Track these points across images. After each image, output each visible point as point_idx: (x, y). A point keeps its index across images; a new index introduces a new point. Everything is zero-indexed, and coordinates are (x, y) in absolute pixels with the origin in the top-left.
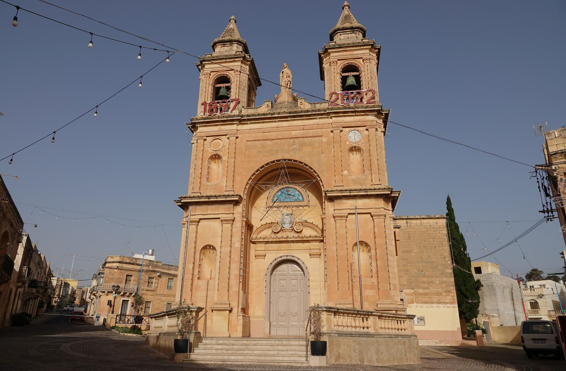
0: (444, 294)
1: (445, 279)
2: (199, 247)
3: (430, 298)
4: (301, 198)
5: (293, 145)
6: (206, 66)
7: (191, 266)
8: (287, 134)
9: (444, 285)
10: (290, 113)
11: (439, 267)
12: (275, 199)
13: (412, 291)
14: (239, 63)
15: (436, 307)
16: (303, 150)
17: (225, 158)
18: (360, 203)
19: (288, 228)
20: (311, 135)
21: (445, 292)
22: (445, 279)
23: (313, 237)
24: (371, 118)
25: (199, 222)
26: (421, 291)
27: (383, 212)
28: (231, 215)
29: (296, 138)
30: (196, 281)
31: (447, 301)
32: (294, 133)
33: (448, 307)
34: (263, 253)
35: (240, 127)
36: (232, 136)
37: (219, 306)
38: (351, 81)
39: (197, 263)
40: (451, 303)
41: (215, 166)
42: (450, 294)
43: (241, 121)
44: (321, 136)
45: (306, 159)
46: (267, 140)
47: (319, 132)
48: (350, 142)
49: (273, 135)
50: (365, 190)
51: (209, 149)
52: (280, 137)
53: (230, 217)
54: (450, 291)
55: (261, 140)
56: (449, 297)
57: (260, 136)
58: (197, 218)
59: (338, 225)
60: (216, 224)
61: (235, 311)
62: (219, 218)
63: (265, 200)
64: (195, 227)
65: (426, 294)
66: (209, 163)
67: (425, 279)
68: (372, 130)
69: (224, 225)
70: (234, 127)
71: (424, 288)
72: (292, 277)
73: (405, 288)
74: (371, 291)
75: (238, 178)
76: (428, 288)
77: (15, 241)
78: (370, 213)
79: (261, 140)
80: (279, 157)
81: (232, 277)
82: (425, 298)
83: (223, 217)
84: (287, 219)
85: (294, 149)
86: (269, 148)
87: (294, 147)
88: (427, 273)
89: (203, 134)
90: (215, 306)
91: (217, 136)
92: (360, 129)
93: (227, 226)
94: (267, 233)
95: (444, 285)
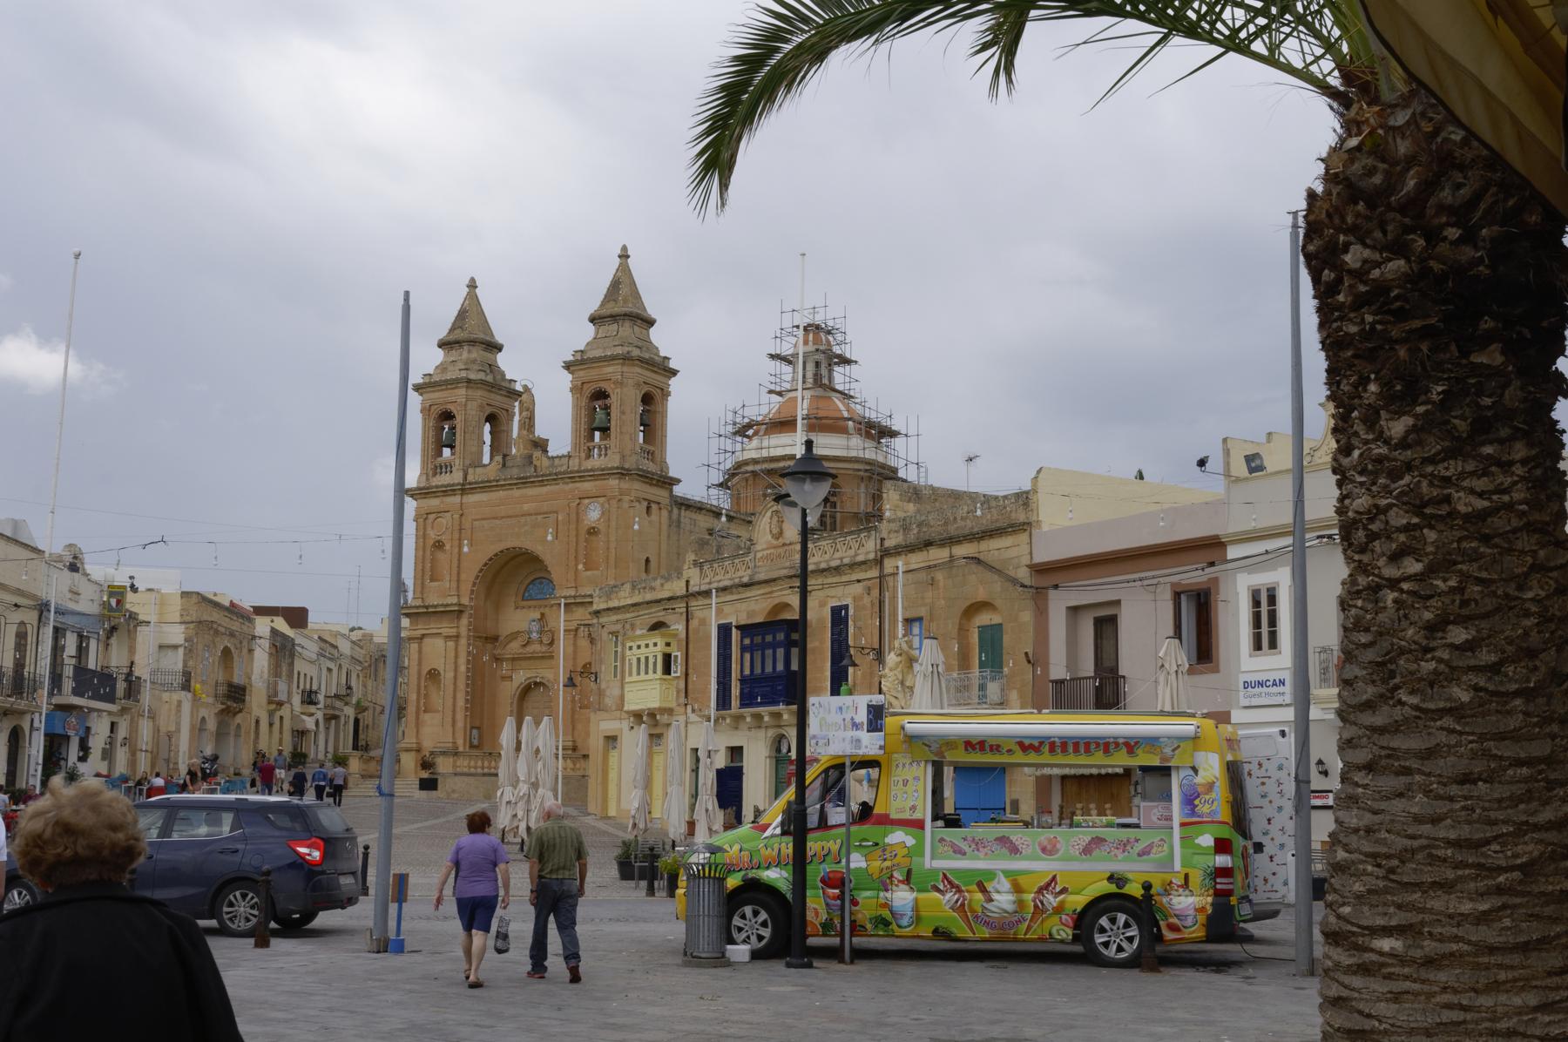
14: (463, 391)
17: (448, 547)
24: (613, 482)
32: (526, 507)
39: (423, 692)
41: (440, 556)
43: (465, 488)
53: (453, 632)
58: (418, 633)
60: (439, 642)
68: (614, 502)
70: (457, 499)
75: (463, 576)
80: (509, 544)
84: (535, 627)
92: (602, 500)
93: (451, 644)
94: (514, 647)
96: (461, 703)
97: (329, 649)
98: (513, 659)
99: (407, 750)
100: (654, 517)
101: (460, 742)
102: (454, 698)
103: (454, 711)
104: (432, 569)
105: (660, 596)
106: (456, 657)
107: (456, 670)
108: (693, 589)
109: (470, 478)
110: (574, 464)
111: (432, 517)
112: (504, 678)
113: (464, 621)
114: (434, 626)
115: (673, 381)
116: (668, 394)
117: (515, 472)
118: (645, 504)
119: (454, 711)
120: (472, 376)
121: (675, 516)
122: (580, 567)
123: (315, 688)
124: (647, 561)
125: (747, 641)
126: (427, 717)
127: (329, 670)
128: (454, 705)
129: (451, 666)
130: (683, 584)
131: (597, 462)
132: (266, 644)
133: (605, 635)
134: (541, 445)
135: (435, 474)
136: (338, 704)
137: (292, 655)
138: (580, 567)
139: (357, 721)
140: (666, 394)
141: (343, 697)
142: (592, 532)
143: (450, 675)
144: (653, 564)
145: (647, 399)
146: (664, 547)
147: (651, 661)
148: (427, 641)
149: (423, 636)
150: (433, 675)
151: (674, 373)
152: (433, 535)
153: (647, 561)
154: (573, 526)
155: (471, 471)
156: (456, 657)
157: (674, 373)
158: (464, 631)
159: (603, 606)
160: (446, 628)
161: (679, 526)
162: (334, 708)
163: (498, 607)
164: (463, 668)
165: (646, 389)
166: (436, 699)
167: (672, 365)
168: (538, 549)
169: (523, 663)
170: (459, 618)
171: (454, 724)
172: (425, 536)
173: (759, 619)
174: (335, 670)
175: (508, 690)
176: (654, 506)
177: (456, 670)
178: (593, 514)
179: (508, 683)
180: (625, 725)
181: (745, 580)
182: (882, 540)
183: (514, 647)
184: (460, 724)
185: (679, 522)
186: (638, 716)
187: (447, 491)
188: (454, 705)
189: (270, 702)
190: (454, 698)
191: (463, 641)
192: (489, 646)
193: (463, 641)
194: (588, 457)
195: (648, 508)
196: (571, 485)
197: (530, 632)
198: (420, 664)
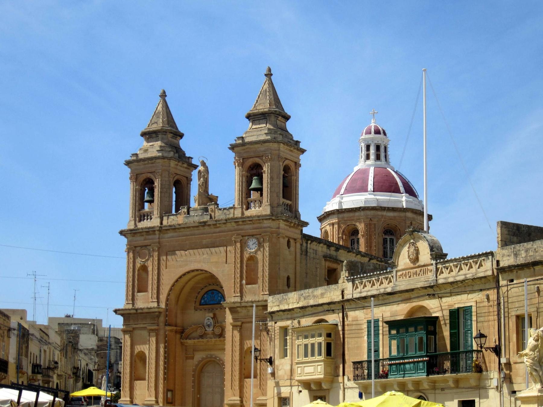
17: (150, 269)
25: (132, 331)
77: (6, 338)
92: (258, 236)
100: (292, 248)
105: (321, 301)
108: (346, 297)
109: (165, 222)
110: (238, 213)
111: (138, 249)
112: (187, 358)
113: (162, 319)
115: (302, 157)
116: (300, 166)
117: (196, 219)
118: (287, 239)
120: (166, 155)
121: (304, 248)
122: (244, 282)
123: (38, 362)
124: (288, 278)
125: (394, 332)
126: (138, 383)
127: (45, 351)
130: (340, 293)
131: (254, 211)
133: (277, 328)
134: (213, 200)
135: (140, 221)
138: (244, 282)
140: (297, 165)
142: (252, 258)
144: (292, 281)
145: (286, 169)
146: (298, 268)
147: (316, 346)
148: (137, 332)
151: (303, 151)
153: (288, 278)
155: (165, 218)
157: (303, 151)
158: (162, 324)
159: (275, 309)
161: (306, 255)
163: (184, 309)
165: (287, 162)
167: (302, 146)
168: (214, 270)
170: (158, 317)
173: (401, 317)
176: (291, 241)
179: (190, 361)
180: (295, 389)
181: (389, 290)
182: (498, 262)
184: (161, 389)
185: (307, 252)
186: (306, 385)
187: (150, 231)
191: (162, 333)
194: (248, 208)
195: (289, 242)
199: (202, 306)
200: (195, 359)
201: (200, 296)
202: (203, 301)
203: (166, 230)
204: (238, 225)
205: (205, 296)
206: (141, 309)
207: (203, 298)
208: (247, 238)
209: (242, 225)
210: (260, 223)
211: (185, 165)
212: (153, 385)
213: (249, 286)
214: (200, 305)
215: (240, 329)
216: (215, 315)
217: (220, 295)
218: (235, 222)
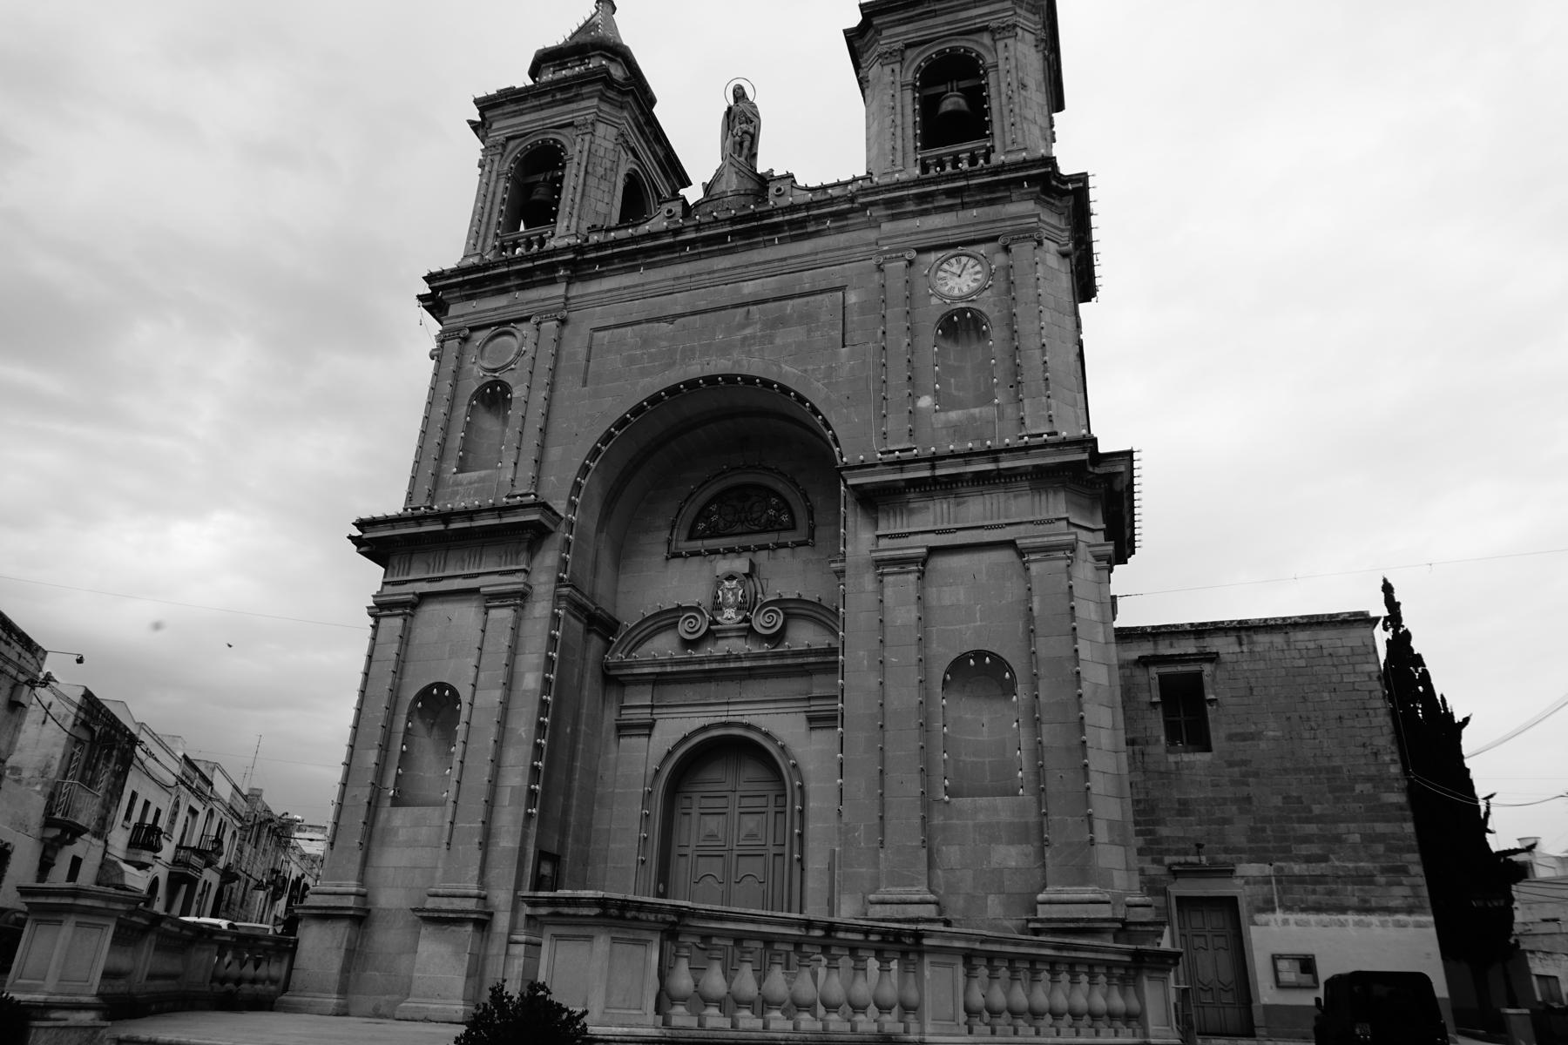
0: (1381, 879)
1: (1381, 827)
2: (410, 693)
3: (1330, 893)
4: (785, 518)
5: (743, 327)
6: (495, 126)
7: (372, 757)
8: (725, 294)
9: (1380, 848)
10: (733, 220)
11: (1359, 788)
12: (701, 526)
13: (1267, 870)
15: (1357, 924)
16: (778, 341)
17: (518, 392)
18: (977, 509)
19: (729, 624)
20: (807, 287)
21: (1384, 871)
22: (1381, 827)
23: (817, 652)
26: (1298, 869)
27: (1060, 534)
28: (520, 578)
29: (756, 303)
30: (385, 810)
31: (1392, 904)
32: (749, 288)
33: (1399, 925)
34: (643, 715)
35: (577, 289)
36: (548, 319)
37: (444, 904)
38: (953, 102)
39: (398, 746)
40: (1410, 911)
41: (489, 422)
42: (1405, 880)
44: (842, 288)
45: (786, 368)
46: (658, 320)
47: (835, 275)
48: (942, 296)
49: (679, 303)
50: (993, 454)
51: (475, 368)
52: (702, 305)
53: (514, 582)
54: (1403, 870)
55: (638, 323)
56: (1397, 891)
57: (637, 309)
59: (888, 592)
60: (466, 614)
61: (502, 921)
62: (476, 591)
63: (666, 534)
64: (398, 621)
65: (1319, 879)
66: (472, 408)
67: (1312, 828)
69: (492, 612)
70: (559, 290)
71: (1308, 859)
72: (746, 802)
73: (1240, 861)
74: (1013, 850)
75: (554, 453)
76: (1325, 859)
78: (1010, 544)
79: (638, 323)
80: (695, 370)
81: (505, 797)
82: (1314, 892)
83: (488, 583)
84: (732, 592)
85: (745, 339)
86: (664, 344)
87: (748, 331)
88: (1317, 809)
89: (460, 323)
90: (431, 903)
91: (503, 327)
92: (982, 249)
93: (502, 615)
94: (664, 646)
95: (1380, 848)
96: (515, 778)
97: (197, 782)
98: (659, 681)
99: (326, 916)
101: (501, 897)
102: (497, 763)
103: (491, 804)
104: (466, 445)
106: (514, 650)
107: (509, 685)
112: (623, 729)
113: (549, 558)
114: (456, 572)
119: (491, 804)
126: (399, 819)
128: (494, 783)
129: (494, 672)
132: (67, 714)
136: (195, 860)
137: (127, 760)
138: (925, 402)
139: (220, 893)
141: (207, 857)
143: (491, 697)
148: (431, 611)
149: (423, 597)
150: (438, 705)
152: (476, 374)
154: (895, 312)
156: (514, 650)
160: (491, 572)
162: (187, 865)
163: (622, 555)
164: (530, 681)
166: (430, 770)
169: (690, 693)
171: (485, 845)
172: (457, 374)
174: (202, 815)
175: (640, 760)
177: (509, 685)
178: (960, 280)
183: (664, 646)
184: (507, 840)
188: (494, 783)
189: (49, 822)
190: (497, 763)
191: (541, 609)
192: (596, 642)
193: (541, 609)
196: (887, 227)
197: (718, 607)
198: (399, 671)
199: (698, 545)
200: (656, 733)
201: (691, 510)
202: (701, 526)
203: (599, 260)
204: (894, 218)
205: (714, 508)
206: (469, 514)
207: (703, 514)
208: (933, 257)
209: (914, 214)
210: (991, 202)
211: (661, 154)
212: (471, 824)
213: (954, 415)
214: (690, 538)
215: (922, 575)
216: (752, 565)
217: (774, 501)
218: (888, 203)
